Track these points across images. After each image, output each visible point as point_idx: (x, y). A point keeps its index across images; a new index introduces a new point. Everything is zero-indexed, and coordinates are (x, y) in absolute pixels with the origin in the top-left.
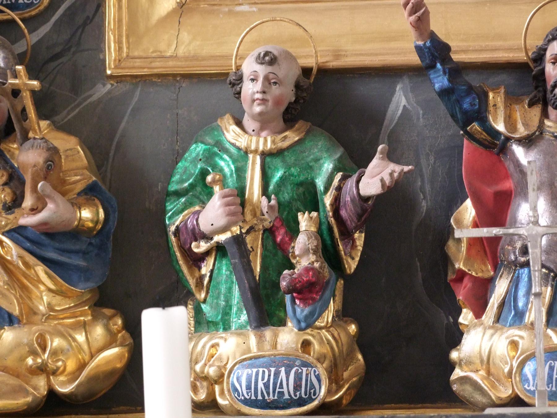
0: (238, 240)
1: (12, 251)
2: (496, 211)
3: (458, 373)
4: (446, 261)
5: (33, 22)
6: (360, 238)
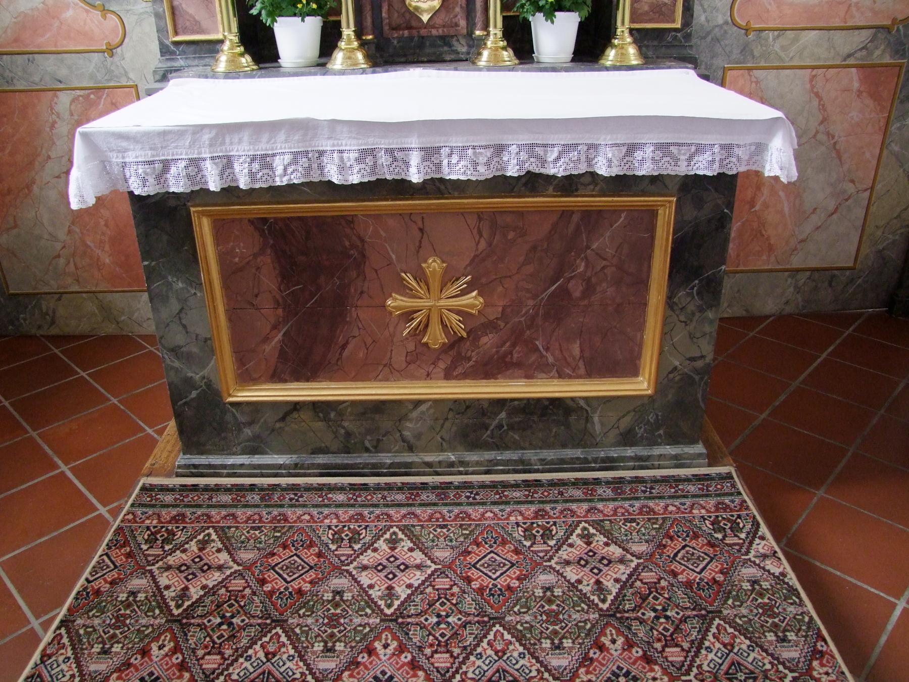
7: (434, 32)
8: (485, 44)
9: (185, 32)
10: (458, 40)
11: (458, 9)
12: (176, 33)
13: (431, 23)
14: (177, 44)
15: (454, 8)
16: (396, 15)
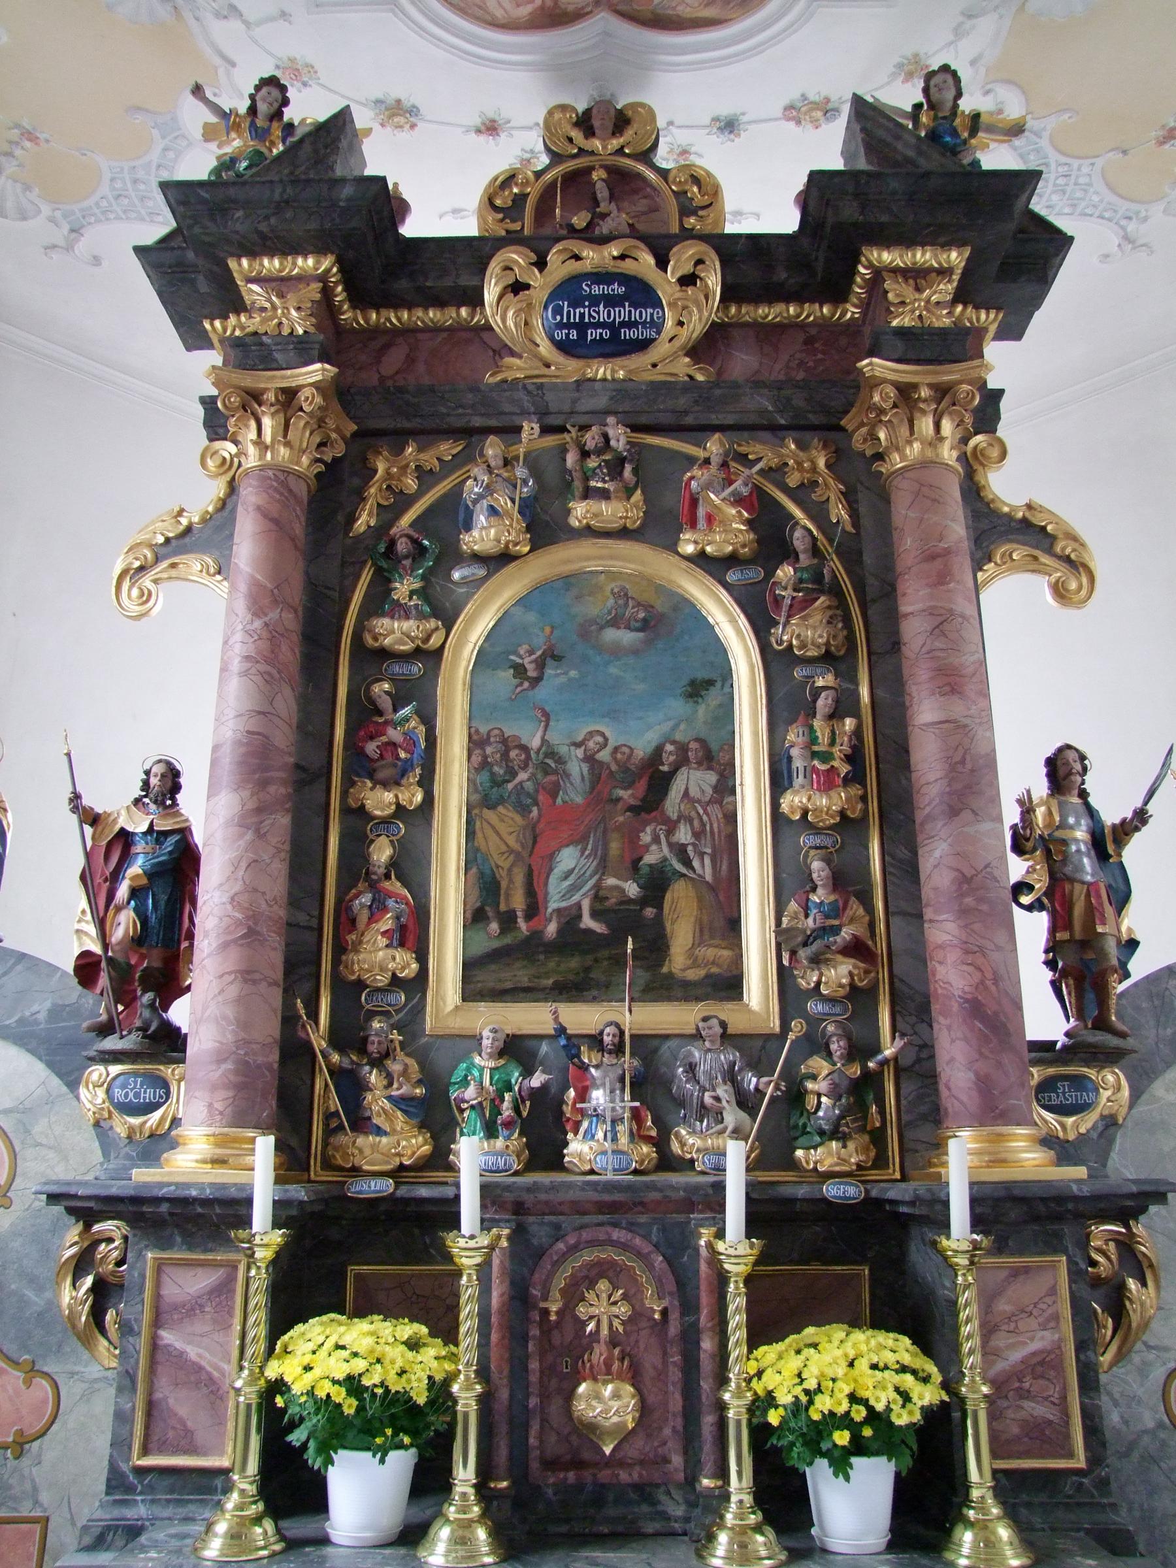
0: (480, 1103)
1: (387, 1105)
2: (583, 1096)
3: (567, 1159)
4: (562, 1113)
5: (397, 1011)
6: (528, 1103)
7: (624, 1476)
8: (722, 1517)
9: (164, 1448)
10: (669, 1493)
11: (667, 1431)
12: (145, 1451)
13: (618, 1456)
14: (141, 1471)
15: (660, 1429)
16: (553, 1438)
